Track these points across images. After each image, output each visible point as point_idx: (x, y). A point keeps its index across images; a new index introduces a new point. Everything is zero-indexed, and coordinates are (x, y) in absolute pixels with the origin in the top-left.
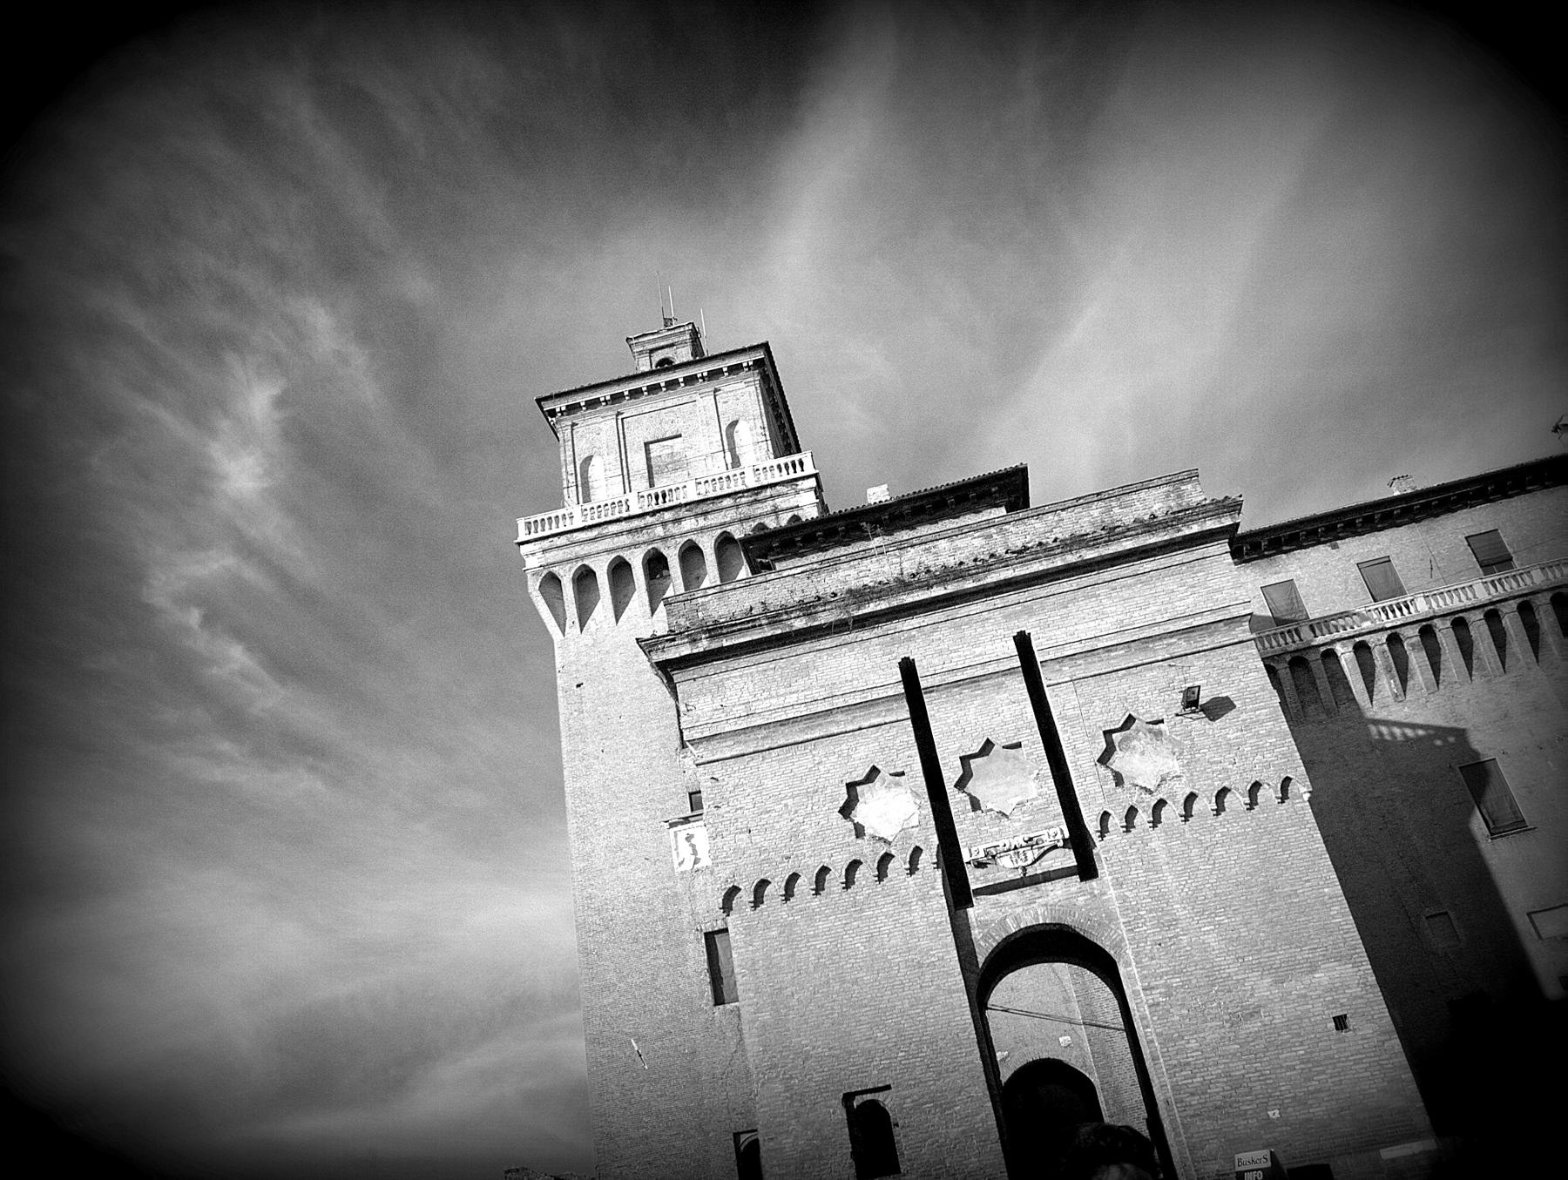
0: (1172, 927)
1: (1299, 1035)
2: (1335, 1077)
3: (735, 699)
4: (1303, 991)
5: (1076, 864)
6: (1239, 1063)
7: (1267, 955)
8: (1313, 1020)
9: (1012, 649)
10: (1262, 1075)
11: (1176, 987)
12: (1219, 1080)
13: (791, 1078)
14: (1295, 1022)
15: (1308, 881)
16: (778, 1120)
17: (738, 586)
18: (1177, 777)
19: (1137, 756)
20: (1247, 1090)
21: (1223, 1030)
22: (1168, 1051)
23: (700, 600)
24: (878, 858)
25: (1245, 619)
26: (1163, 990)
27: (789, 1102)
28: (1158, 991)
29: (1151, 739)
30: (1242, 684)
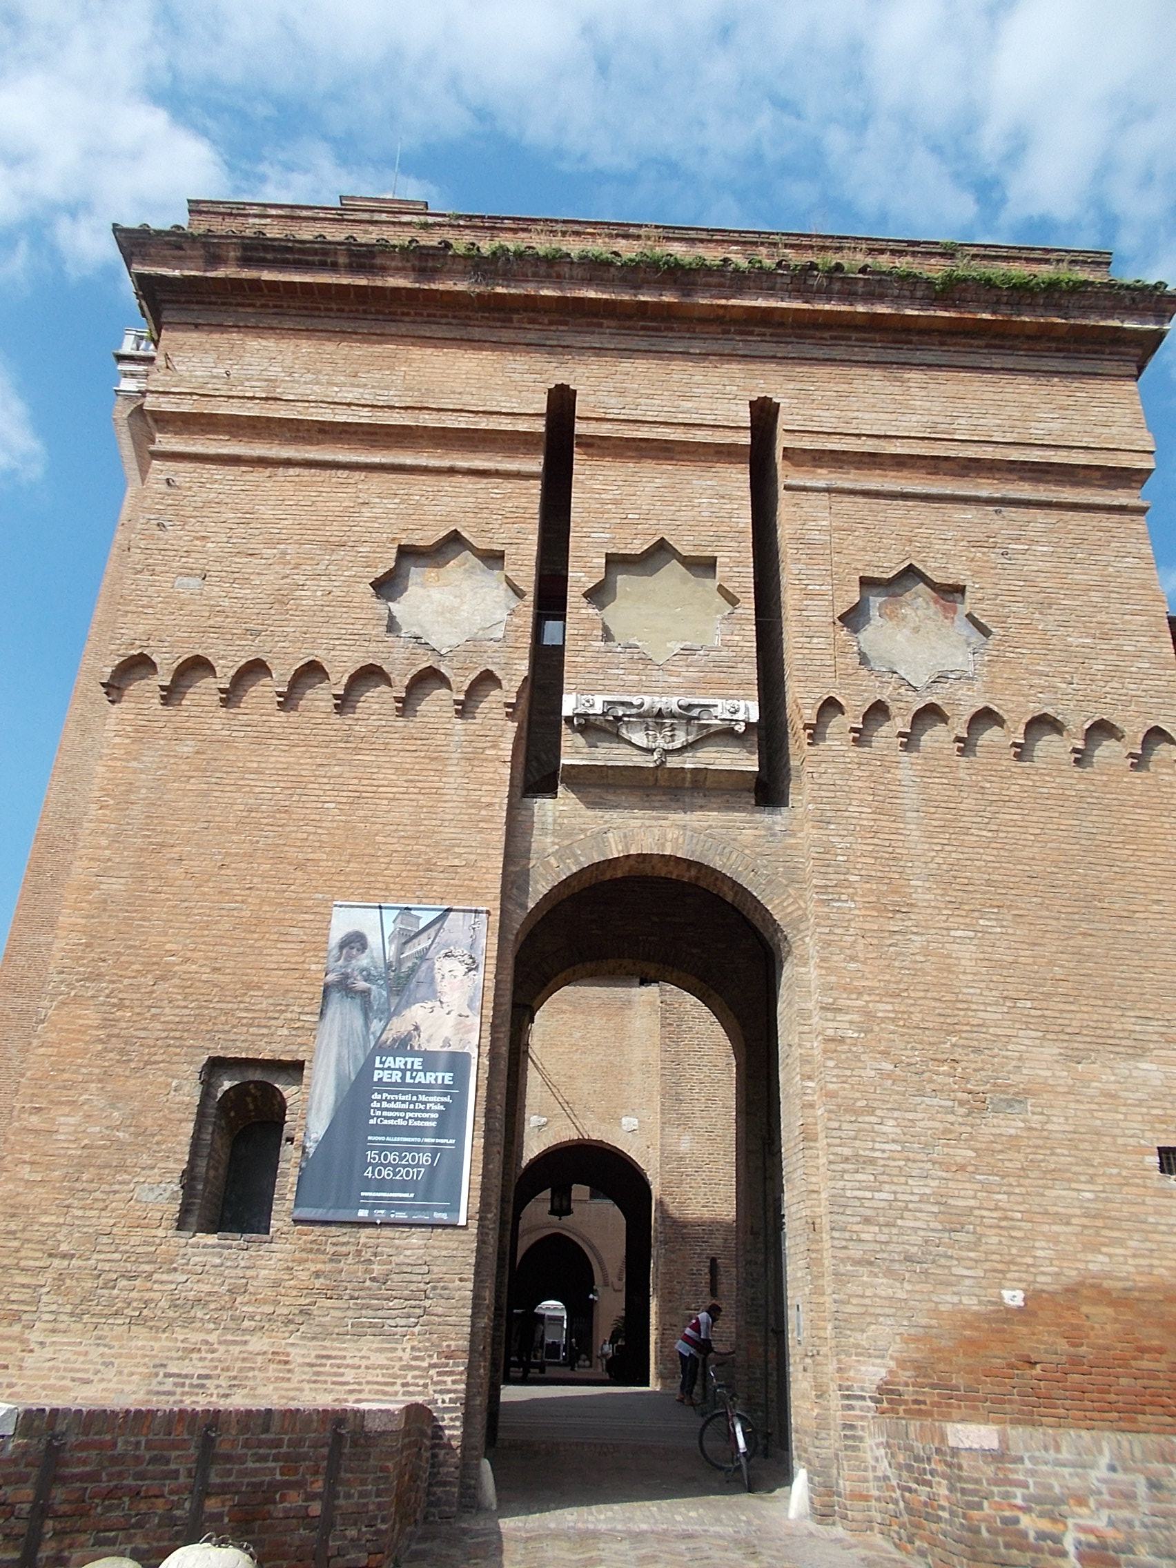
0: (898, 916)
1: (1088, 1163)
2: (1143, 1256)
3: (254, 371)
4: (1112, 1087)
5: (757, 769)
6: (967, 1185)
7: (1062, 1006)
8: (1120, 1141)
9: (744, 416)
10: (1006, 1218)
11: (883, 1020)
12: (922, 1206)
13: (120, 1006)
14: (1087, 1137)
15: (1158, 902)
16: (66, 1076)
17: (321, 215)
18: (968, 678)
19: (906, 631)
20: (971, 1238)
21: (951, 1118)
22: (839, 1129)
23: (251, 221)
24: (414, 671)
25: (1138, 478)
26: (856, 1018)
27: (100, 1047)
28: (848, 1017)
29: (936, 613)
30: (1111, 569)
